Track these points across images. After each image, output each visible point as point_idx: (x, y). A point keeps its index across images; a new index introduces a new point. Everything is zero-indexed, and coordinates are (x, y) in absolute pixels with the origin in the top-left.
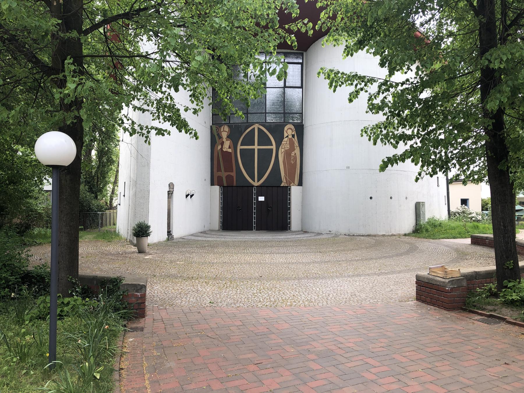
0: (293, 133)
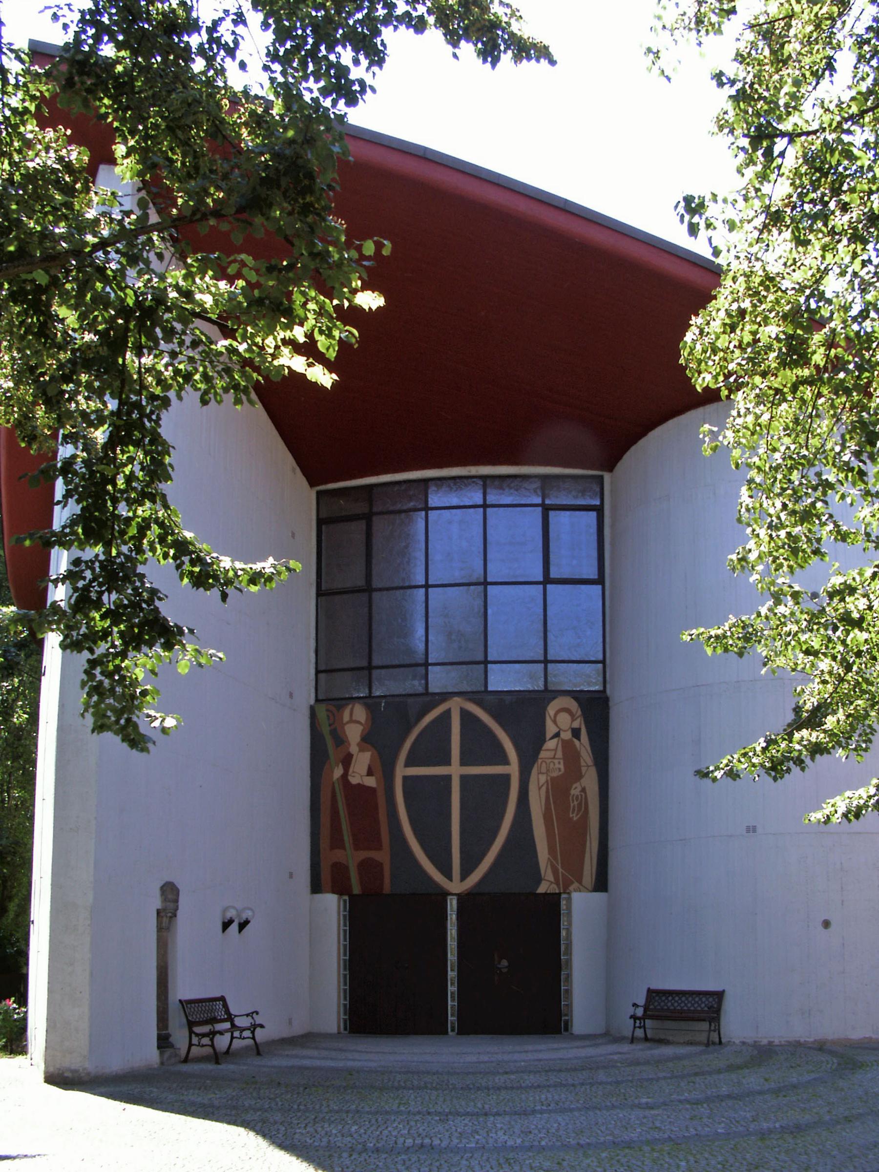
0: (576, 725)
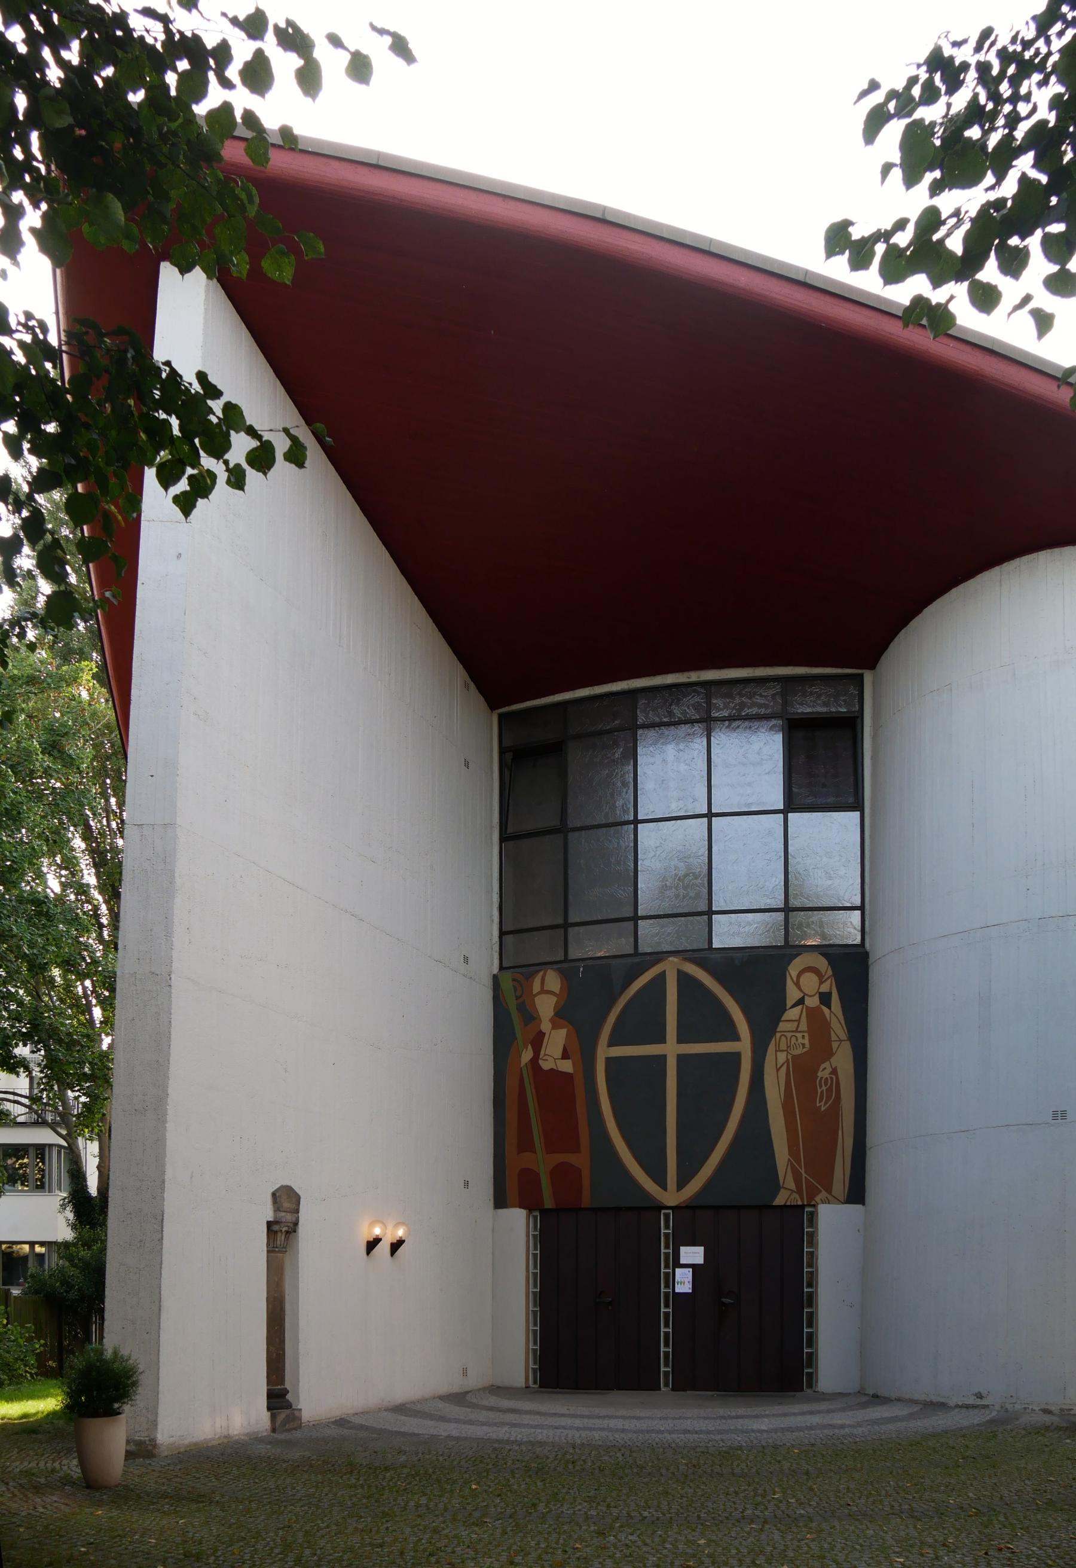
0: (825, 988)
